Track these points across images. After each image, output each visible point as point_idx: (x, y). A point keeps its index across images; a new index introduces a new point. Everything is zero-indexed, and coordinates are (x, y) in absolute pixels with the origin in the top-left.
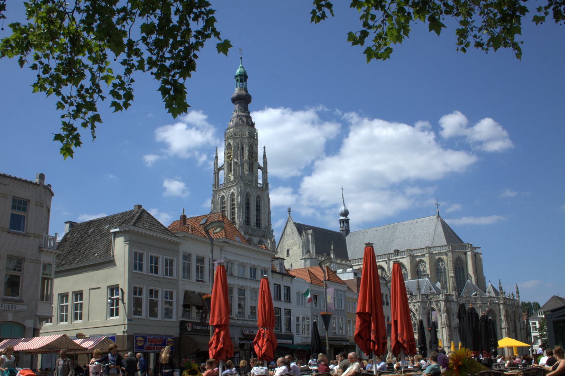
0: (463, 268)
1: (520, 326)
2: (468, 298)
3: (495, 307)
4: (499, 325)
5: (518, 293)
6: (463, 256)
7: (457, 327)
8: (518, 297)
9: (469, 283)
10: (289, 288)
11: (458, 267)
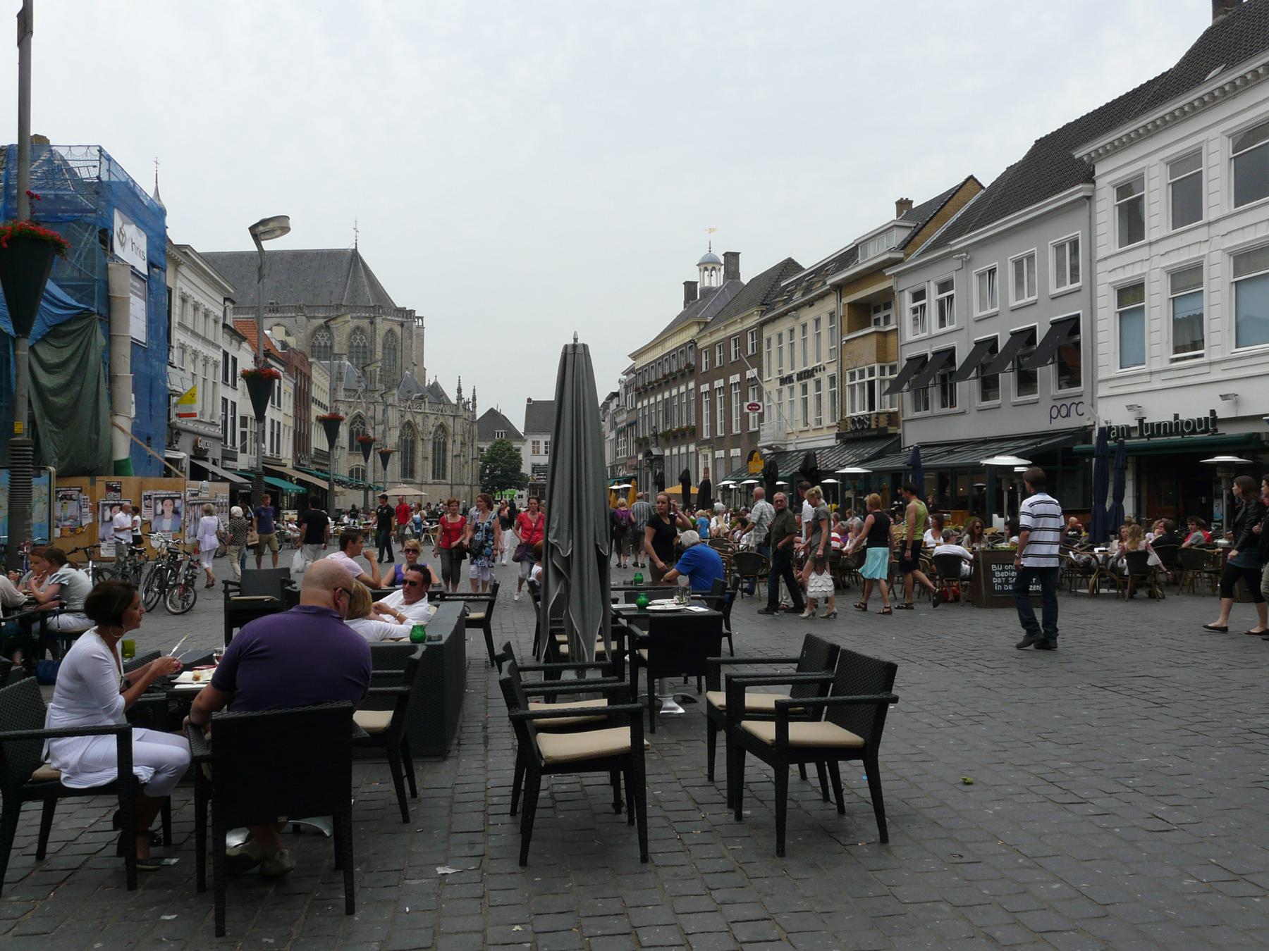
0: (395, 349)
5: (474, 399)
6: (398, 329)
8: (474, 406)
10: (235, 360)
11: (387, 346)
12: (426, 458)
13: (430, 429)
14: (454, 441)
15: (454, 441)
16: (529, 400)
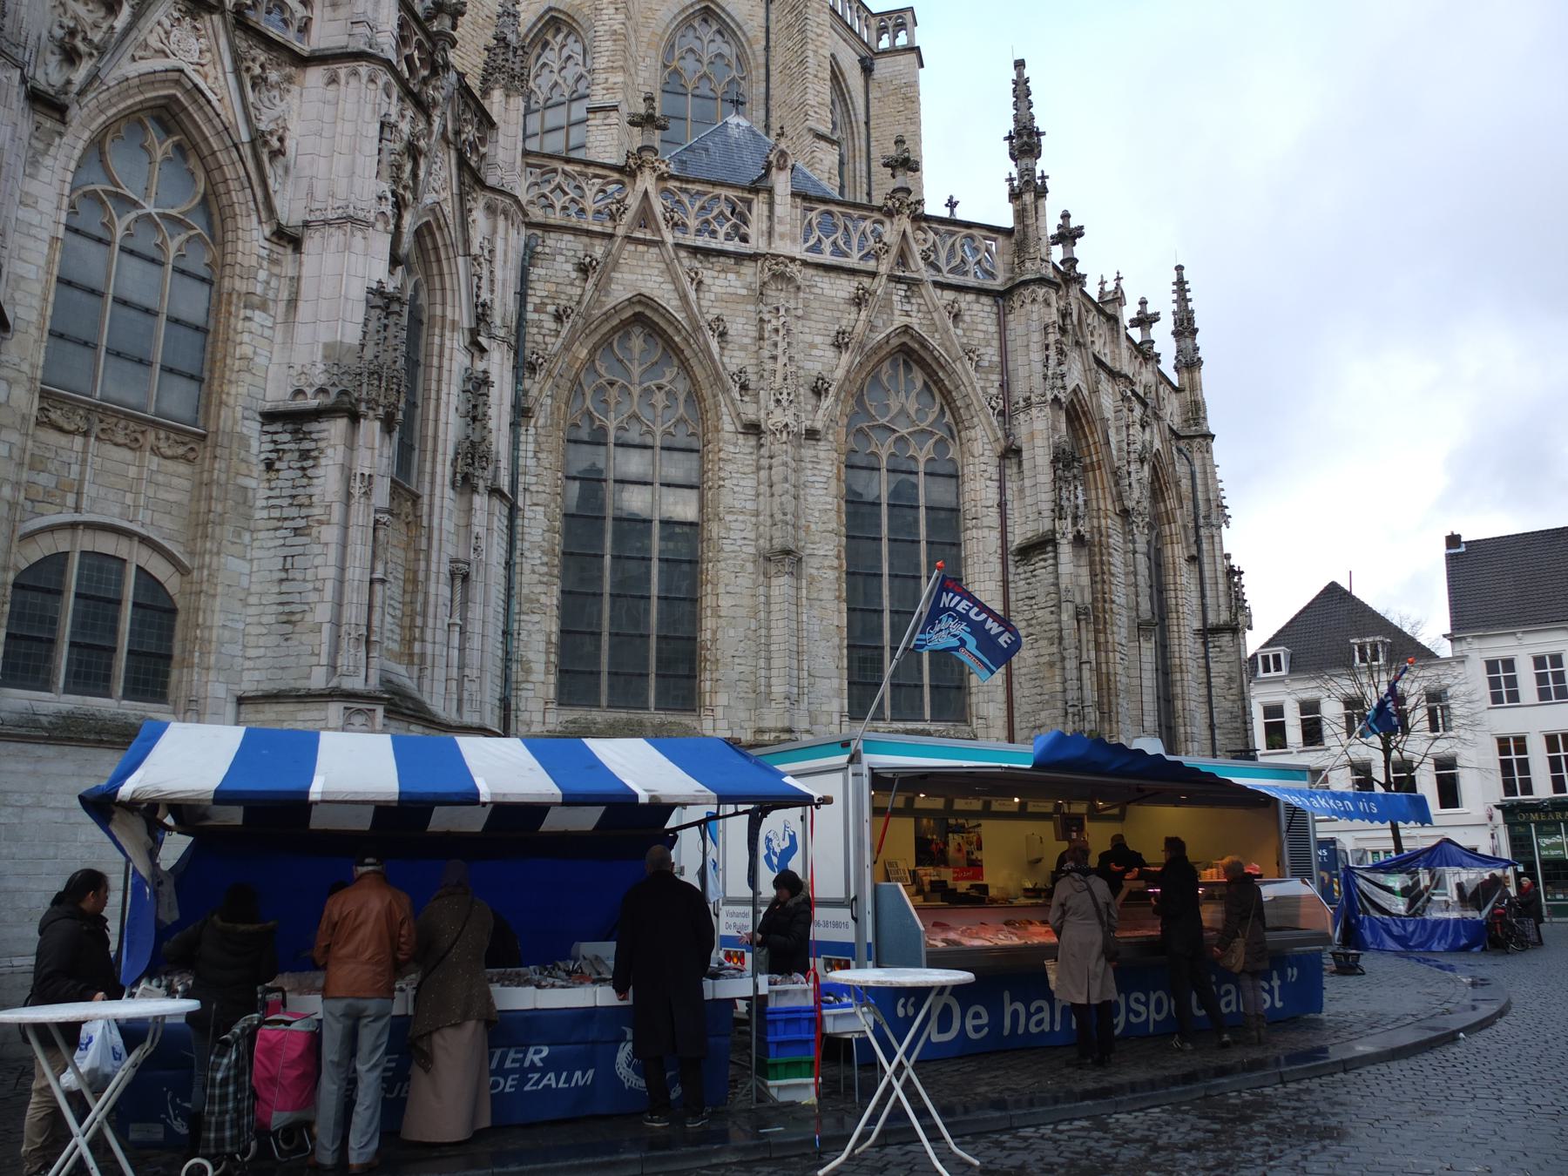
1: (1204, 606)
2: (646, 181)
3: (957, 317)
4: (993, 518)
7: (312, 403)
9: (734, 132)
12: (786, 558)
13: (814, 367)
14: (1011, 453)
15: (1011, 453)
16: (1453, 540)
